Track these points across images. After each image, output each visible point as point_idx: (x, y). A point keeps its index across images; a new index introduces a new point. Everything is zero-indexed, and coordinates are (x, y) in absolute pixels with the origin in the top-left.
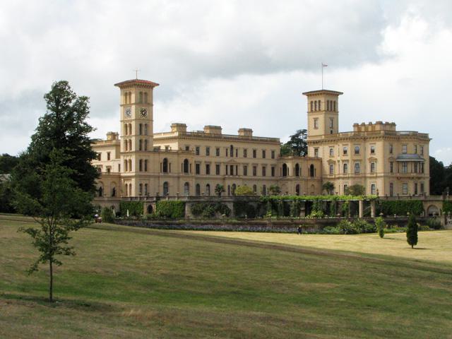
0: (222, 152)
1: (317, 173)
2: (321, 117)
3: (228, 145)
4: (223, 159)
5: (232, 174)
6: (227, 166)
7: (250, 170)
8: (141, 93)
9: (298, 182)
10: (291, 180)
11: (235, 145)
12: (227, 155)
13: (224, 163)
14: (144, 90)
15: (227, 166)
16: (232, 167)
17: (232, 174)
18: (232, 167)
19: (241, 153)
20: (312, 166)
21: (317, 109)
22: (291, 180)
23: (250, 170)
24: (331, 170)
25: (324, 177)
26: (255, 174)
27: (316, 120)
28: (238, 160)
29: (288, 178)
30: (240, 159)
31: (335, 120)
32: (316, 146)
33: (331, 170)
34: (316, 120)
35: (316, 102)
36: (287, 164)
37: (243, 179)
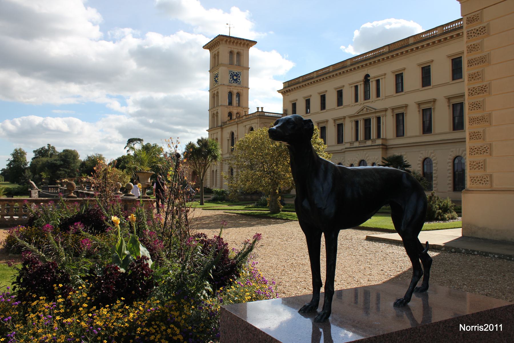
0: (348, 96)
3: (358, 77)
4: (350, 108)
5: (367, 136)
6: (357, 122)
7: (413, 122)
8: (231, 53)
11: (374, 72)
12: (356, 100)
13: (350, 117)
14: (236, 49)
15: (357, 122)
16: (367, 122)
17: (367, 136)
18: (367, 122)
19: (388, 85)
26: (427, 129)
30: (388, 100)
37: (385, 147)
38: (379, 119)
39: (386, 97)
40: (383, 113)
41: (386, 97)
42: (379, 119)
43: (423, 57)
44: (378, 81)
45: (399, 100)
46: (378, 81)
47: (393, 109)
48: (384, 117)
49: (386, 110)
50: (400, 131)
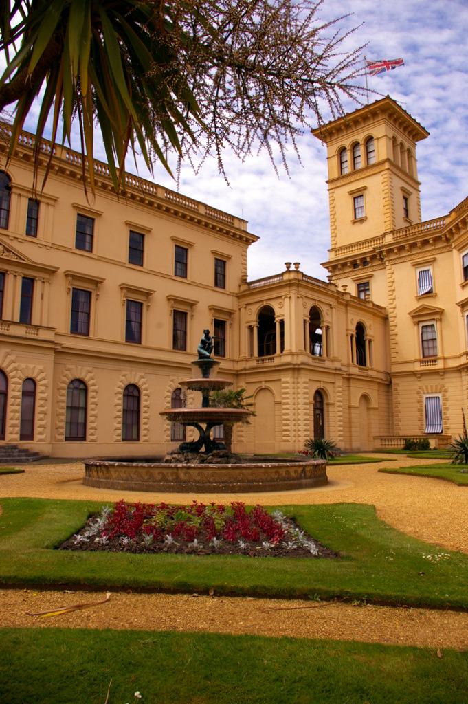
1: (375, 353)
2: (378, 187)
9: (322, 381)
10: (296, 369)
19: (59, 224)
20: (360, 328)
21: (361, 164)
22: (296, 369)
23: (108, 318)
24: (427, 343)
25: (395, 369)
27: (357, 195)
28: (34, 253)
29: (278, 360)
31: (412, 199)
32: (362, 273)
33: (427, 343)
34: (357, 195)
35: (355, 145)
36: (275, 305)
38: (28, 285)
39: (54, 247)
40: (47, 276)
41: (54, 247)
42: (28, 285)
43: (142, 218)
44: (34, 205)
45: (83, 265)
46: (34, 205)
47: (67, 275)
48: (47, 284)
49: (52, 272)
50: (80, 321)
